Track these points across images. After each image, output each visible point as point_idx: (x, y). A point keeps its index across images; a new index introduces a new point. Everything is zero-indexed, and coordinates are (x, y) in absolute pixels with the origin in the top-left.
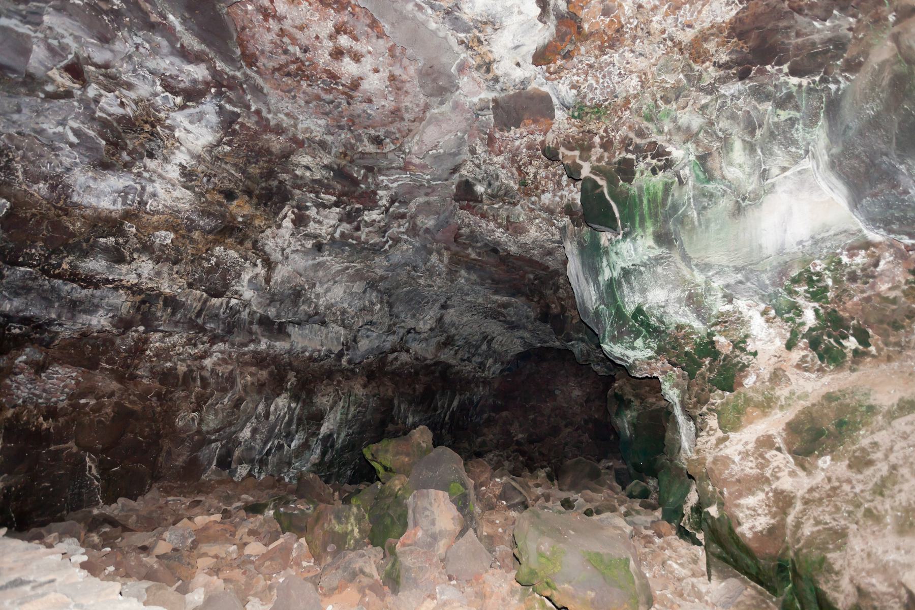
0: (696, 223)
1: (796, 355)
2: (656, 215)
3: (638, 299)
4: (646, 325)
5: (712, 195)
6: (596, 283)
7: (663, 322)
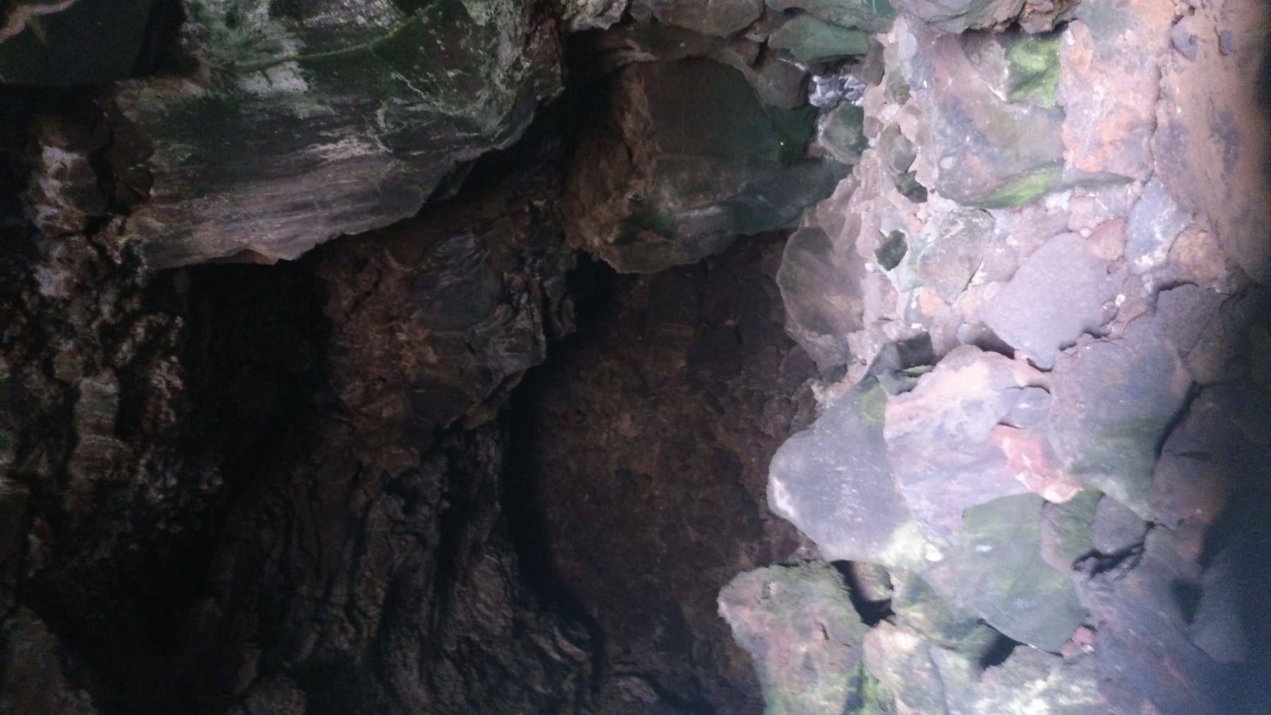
6: (315, 129)
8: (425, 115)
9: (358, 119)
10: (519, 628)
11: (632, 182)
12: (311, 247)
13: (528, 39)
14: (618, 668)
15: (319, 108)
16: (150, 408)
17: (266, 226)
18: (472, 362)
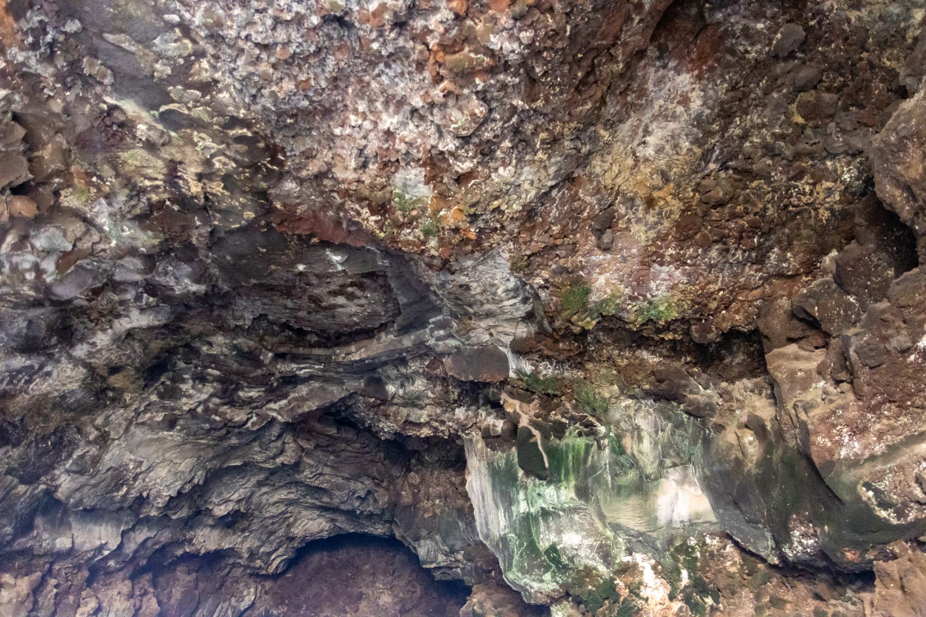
2: (578, 472)
3: (553, 538)
4: (556, 561)
5: (623, 466)
6: (508, 510)
8: (513, 552)
10: (292, 539)
14: (260, 587)
15: (515, 514)
17: (477, 482)
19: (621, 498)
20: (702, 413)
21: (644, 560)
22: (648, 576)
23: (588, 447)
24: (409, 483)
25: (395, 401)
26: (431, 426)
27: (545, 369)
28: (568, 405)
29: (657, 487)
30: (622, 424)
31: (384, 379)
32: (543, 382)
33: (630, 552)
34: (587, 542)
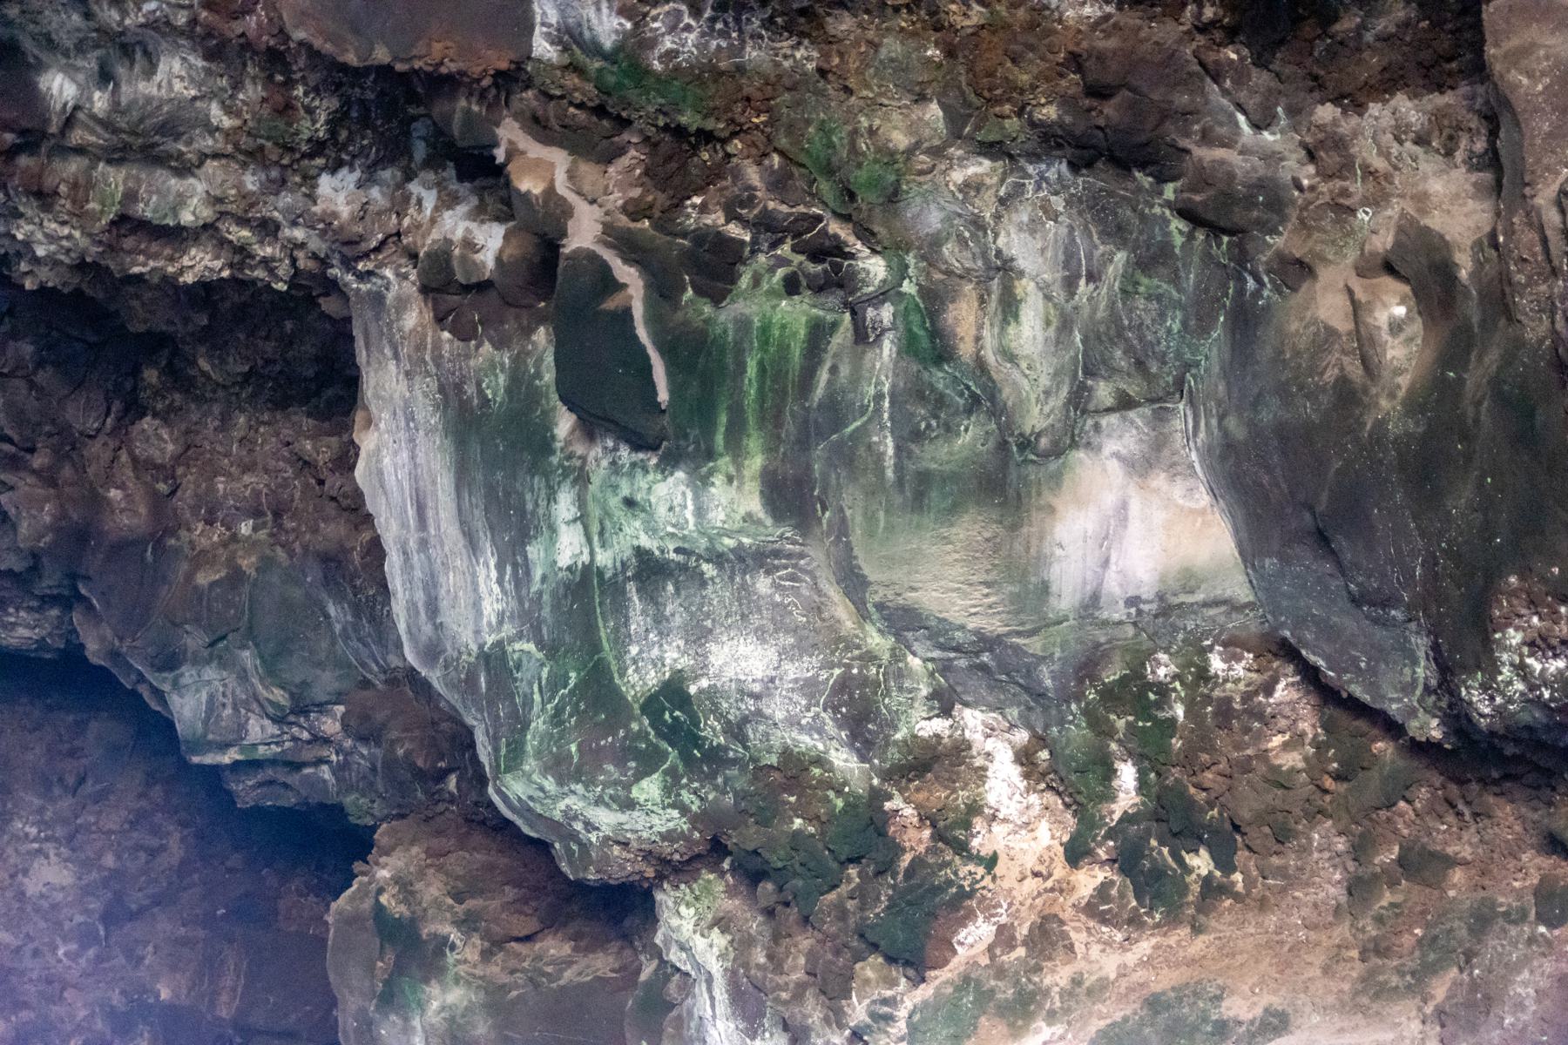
0: (890, 473)
1: (1088, 880)
2: (778, 422)
3: (674, 655)
4: (684, 736)
5: (940, 401)
6: (513, 559)
7: (742, 739)
8: (528, 702)
9: (527, 618)
11: (476, 940)
12: (370, 507)
13: (625, 844)
15: (538, 574)
16: (155, 247)
17: (399, 454)
18: (194, 640)
19: (928, 520)
20: (1238, 216)
21: (990, 731)
22: (1003, 784)
23: (819, 333)
24: (135, 460)
25: (77, 136)
26: (223, 243)
27: (672, 29)
28: (753, 175)
29: (1056, 479)
30: (947, 249)
31: (28, 44)
32: (663, 81)
33: (944, 703)
34: (792, 671)
